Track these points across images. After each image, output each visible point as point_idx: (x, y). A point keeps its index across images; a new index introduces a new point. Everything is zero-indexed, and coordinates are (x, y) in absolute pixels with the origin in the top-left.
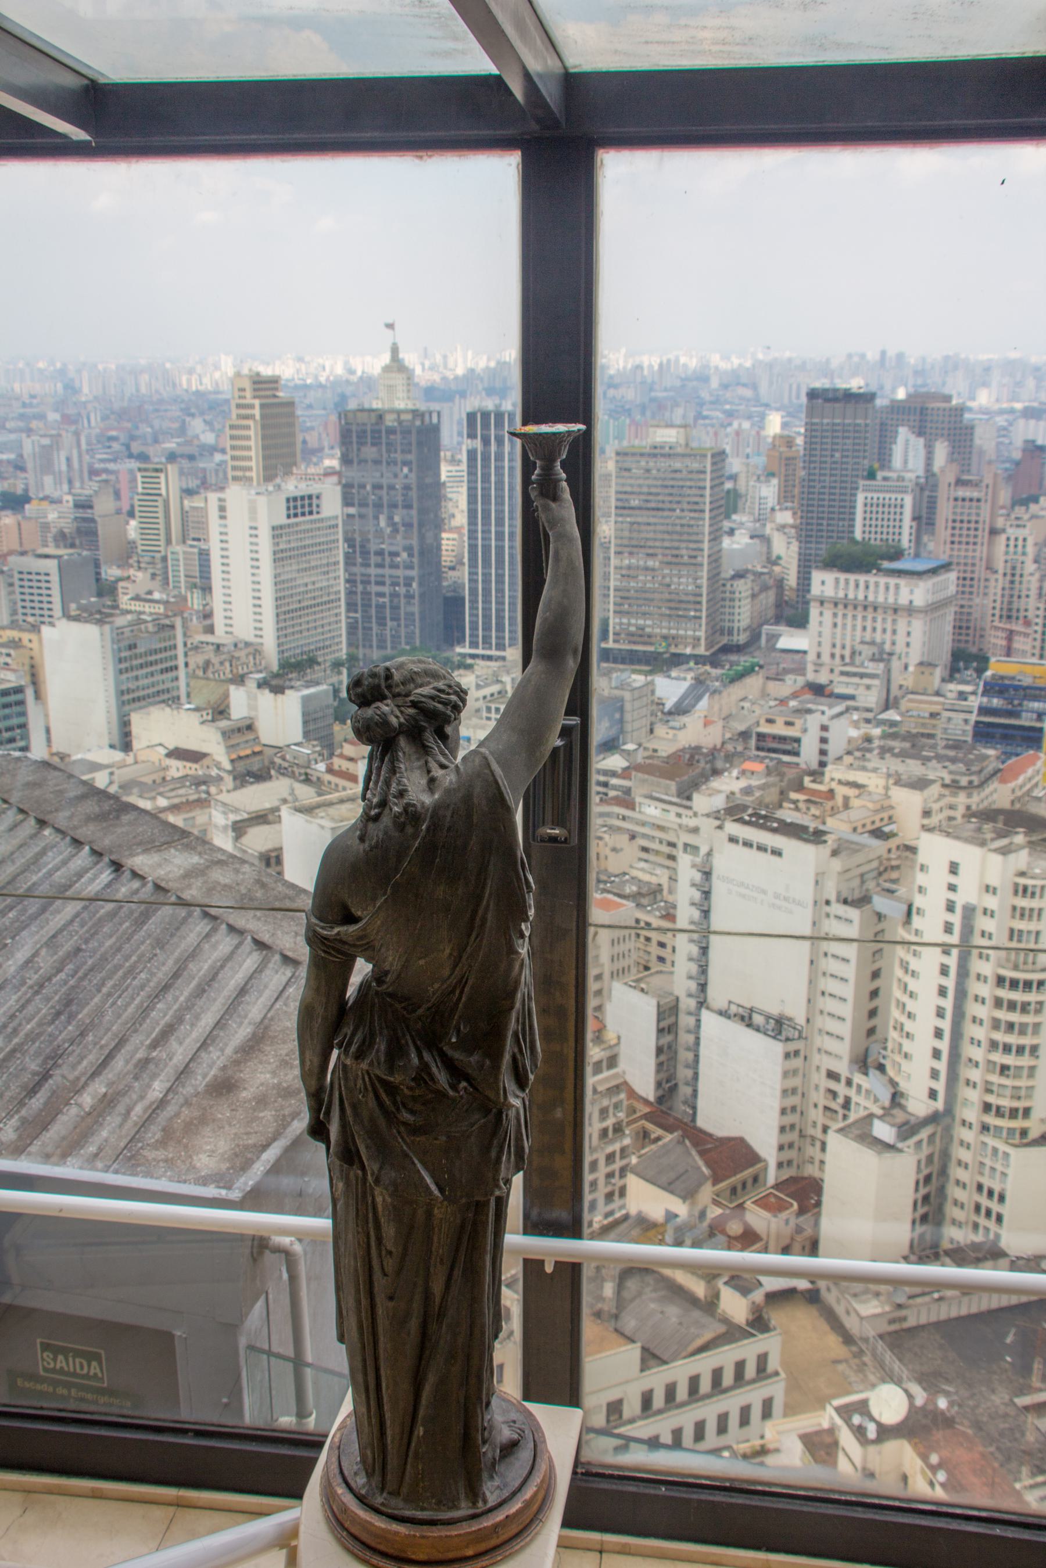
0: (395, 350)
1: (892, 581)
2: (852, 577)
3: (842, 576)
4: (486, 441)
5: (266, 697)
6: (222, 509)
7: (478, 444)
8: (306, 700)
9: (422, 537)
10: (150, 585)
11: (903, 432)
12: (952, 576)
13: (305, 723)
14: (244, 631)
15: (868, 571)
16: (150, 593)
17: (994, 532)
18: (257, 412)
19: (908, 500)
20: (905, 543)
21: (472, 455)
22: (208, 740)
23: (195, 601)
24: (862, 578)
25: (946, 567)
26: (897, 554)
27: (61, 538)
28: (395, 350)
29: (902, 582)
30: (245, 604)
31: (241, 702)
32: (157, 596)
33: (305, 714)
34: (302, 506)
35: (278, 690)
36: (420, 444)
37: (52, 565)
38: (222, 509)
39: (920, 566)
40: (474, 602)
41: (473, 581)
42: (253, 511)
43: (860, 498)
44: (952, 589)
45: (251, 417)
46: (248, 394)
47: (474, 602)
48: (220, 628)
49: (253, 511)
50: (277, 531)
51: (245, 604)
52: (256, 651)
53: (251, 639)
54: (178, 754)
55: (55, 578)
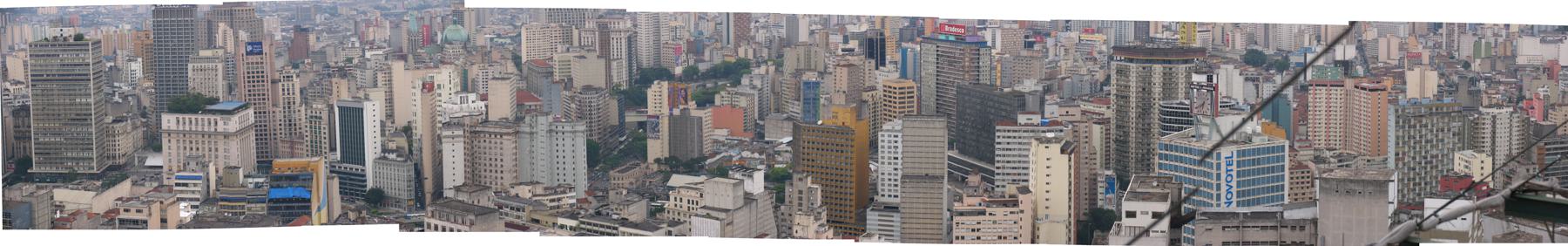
1: (212, 118)
2: (187, 116)
3: (181, 116)
11: (222, 26)
12: (251, 111)
15: (196, 112)
17: (274, 82)
19: (220, 66)
20: (220, 95)
24: (193, 117)
25: (245, 107)
26: (215, 101)
29: (218, 118)
39: (230, 107)
43: (190, 66)
44: (252, 120)
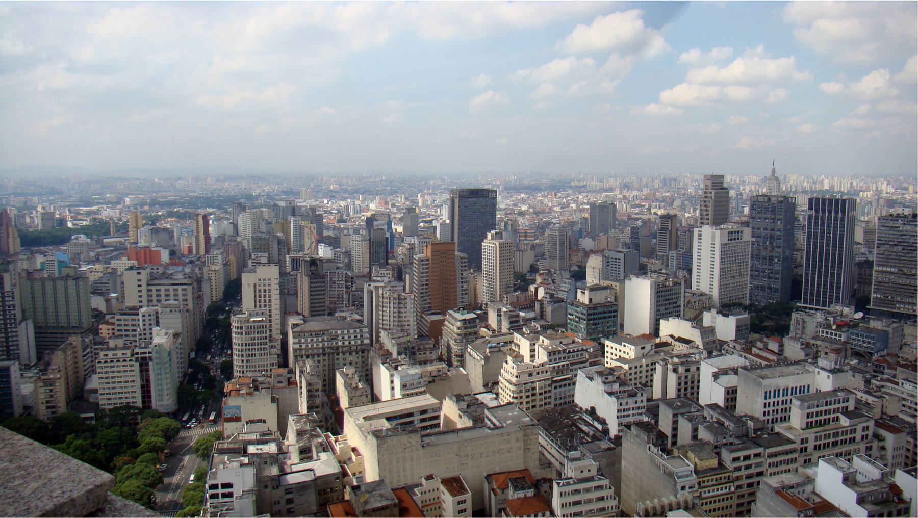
0: (774, 171)
4: (817, 211)
5: (720, 318)
6: (700, 235)
7: (813, 212)
8: (738, 321)
9: (784, 252)
10: (661, 267)
13: (737, 331)
14: (704, 288)
16: (661, 270)
18: (713, 195)
21: (810, 217)
22: (694, 335)
23: (682, 274)
27: (625, 245)
28: (774, 171)
30: (706, 276)
31: (708, 318)
32: (664, 271)
33: (737, 327)
34: (734, 236)
35: (726, 315)
36: (786, 211)
37: (621, 256)
38: (700, 235)
40: (807, 282)
41: (807, 274)
42: (713, 237)
45: (711, 197)
46: (710, 187)
47: (807, 282)
48: (694, 287)
49: (713, 237)
50: (723, 245)
51: (706, 276)
52: (710, 298)
53: (708, 292)
54: (681, 340)
55: (622, 261)
